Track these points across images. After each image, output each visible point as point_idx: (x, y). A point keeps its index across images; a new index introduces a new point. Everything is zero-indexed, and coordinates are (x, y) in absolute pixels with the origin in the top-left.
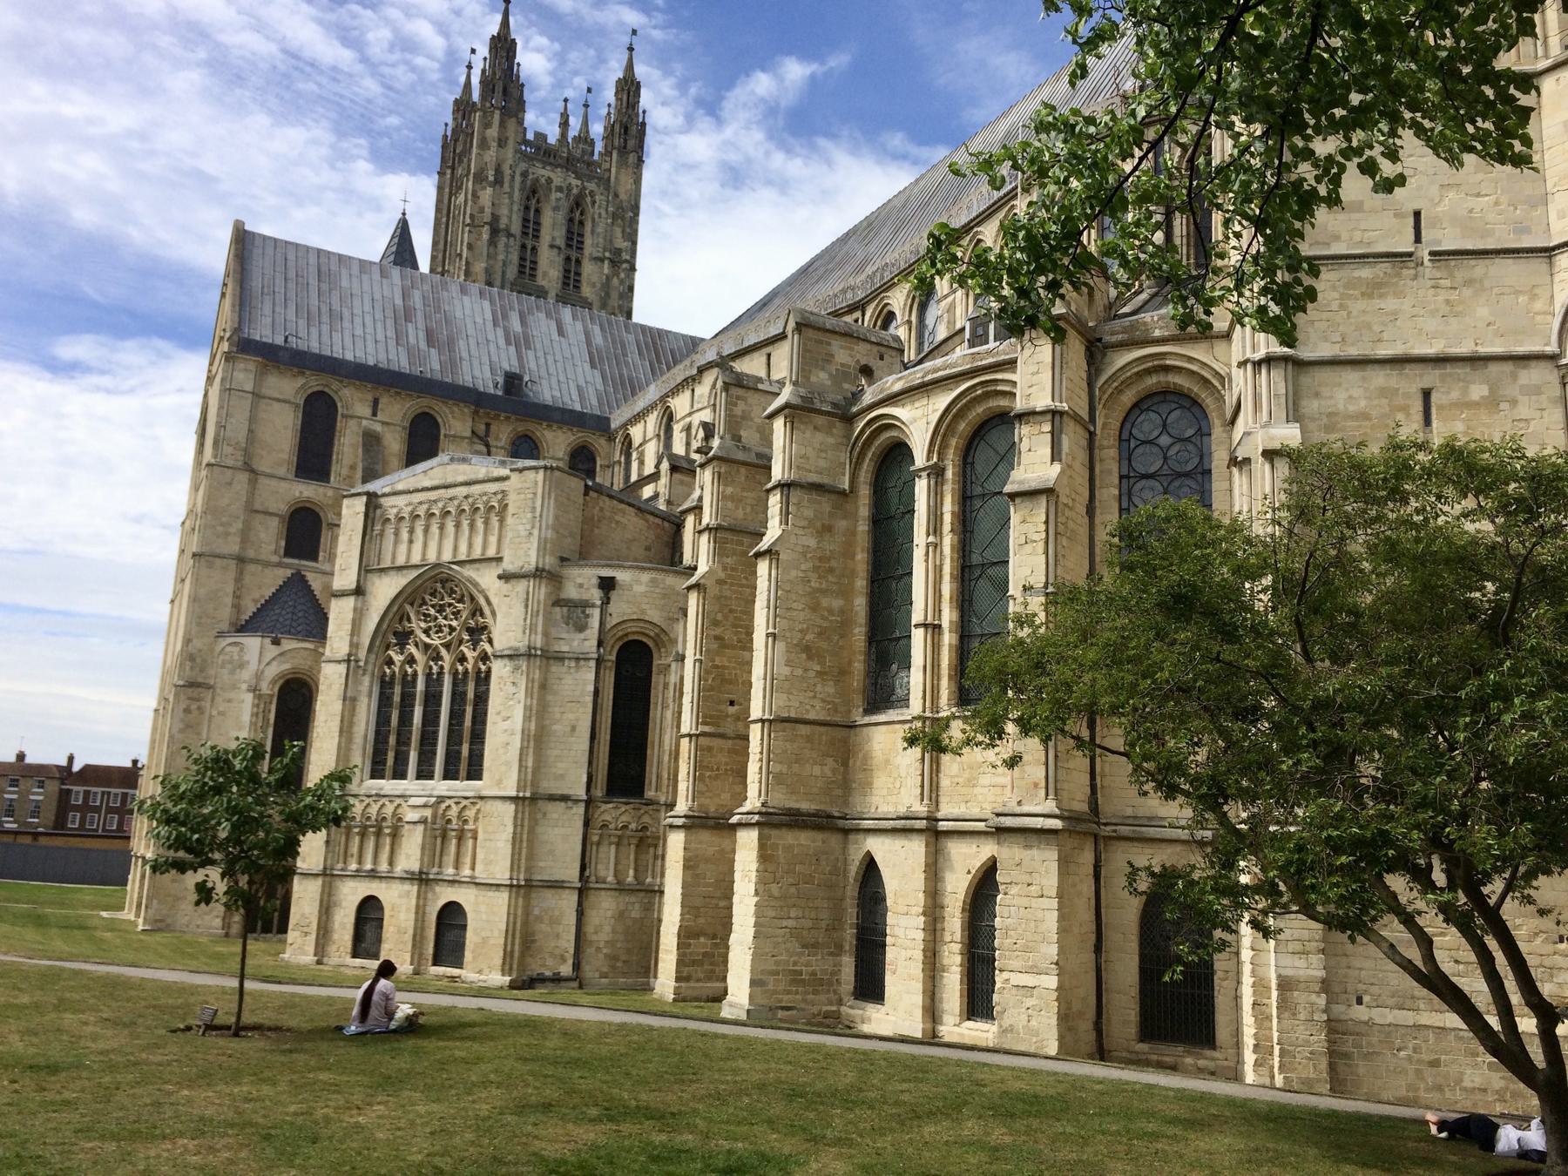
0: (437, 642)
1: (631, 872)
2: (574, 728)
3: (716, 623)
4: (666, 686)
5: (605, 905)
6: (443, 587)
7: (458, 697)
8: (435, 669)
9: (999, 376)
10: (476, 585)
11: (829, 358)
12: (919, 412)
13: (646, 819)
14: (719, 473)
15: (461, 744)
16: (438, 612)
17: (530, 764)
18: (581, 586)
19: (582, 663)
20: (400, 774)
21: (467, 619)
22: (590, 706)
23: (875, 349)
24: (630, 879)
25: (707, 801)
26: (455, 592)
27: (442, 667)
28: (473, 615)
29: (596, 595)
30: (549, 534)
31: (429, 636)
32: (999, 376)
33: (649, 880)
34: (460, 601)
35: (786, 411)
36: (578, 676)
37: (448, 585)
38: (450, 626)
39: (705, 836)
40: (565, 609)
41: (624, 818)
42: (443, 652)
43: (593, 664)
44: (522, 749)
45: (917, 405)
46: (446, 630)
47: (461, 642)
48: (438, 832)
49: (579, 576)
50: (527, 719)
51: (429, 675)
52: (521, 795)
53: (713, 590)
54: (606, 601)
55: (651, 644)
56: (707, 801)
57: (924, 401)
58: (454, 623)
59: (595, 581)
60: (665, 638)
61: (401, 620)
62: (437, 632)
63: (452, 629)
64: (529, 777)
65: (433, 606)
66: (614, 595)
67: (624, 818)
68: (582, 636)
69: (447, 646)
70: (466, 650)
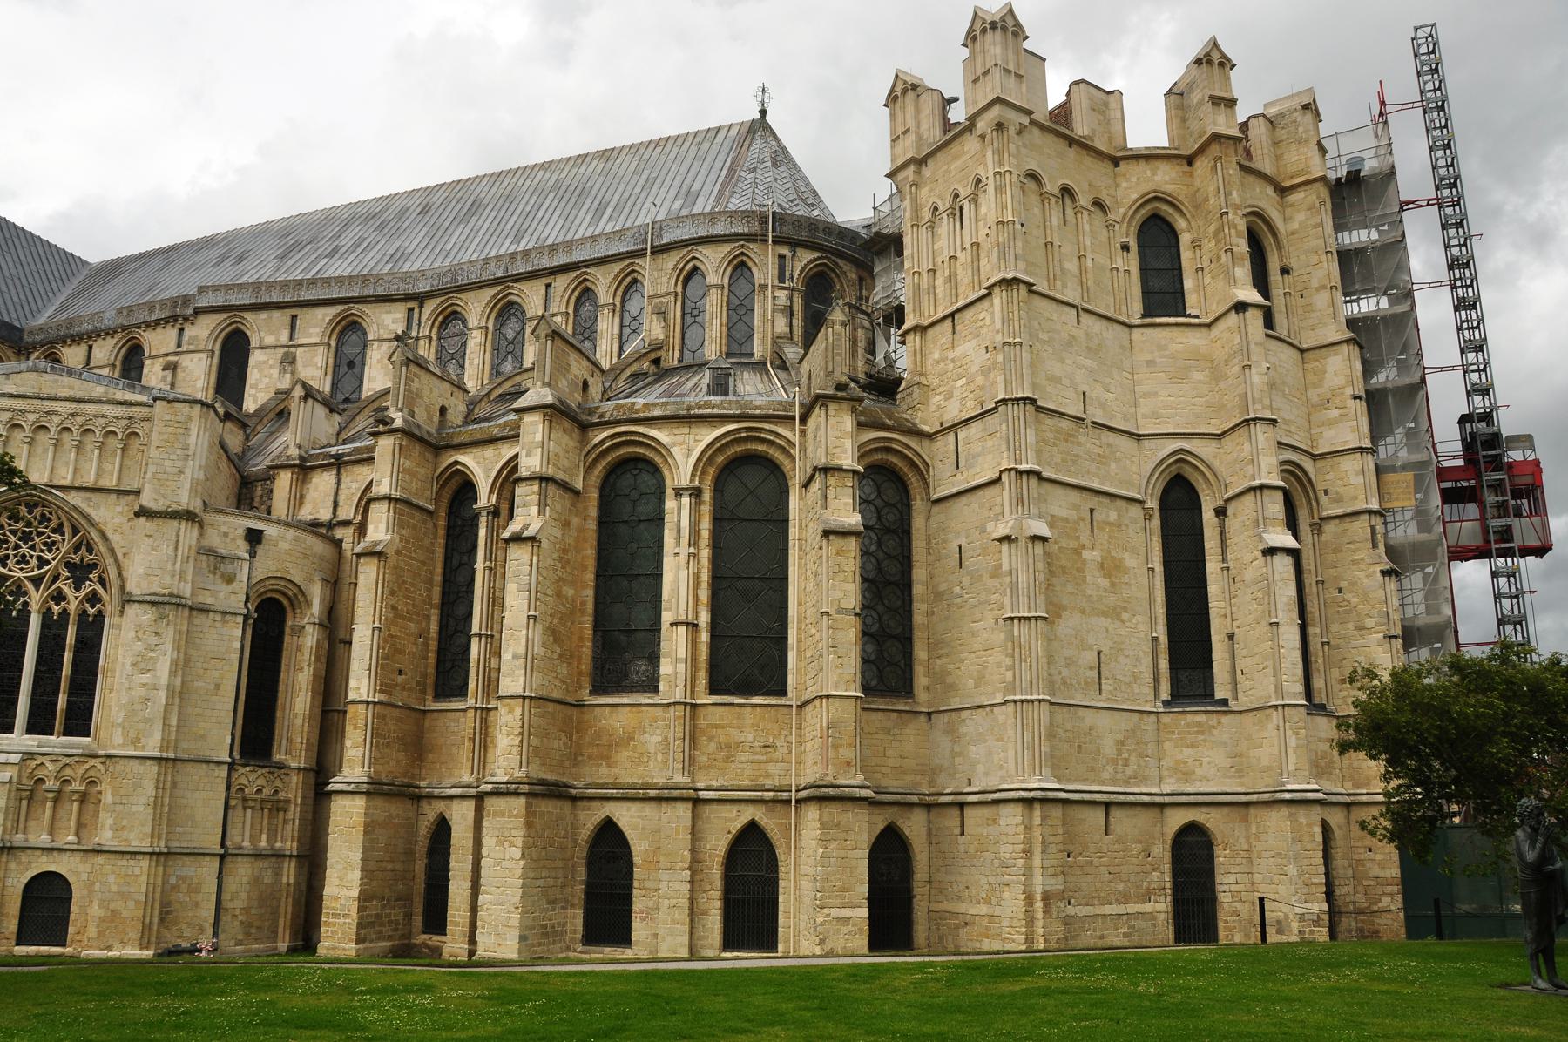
0: (21, 574)
1: (264, 837)
2: (218, 686)
3: (392, 593)
4: (299, 648)
5: (242, 871)
6: (30, 512)
9: (766, 426)
10: (87, 517)
11: (567, 368)
12: (679, 439)
13: (278, 783)
14: (401, 446)
15: (57, 693)
16: (20, 539)
17: (174, 722)
19: (228, 617)
21: (67, 552)
22: (236, 664)
23: (591, 366)
24: (263, 844)
25: (380, 768)
26: (49, 520)
27: (26, 604)
28: (77, 548)
29: (242, 549)
30: (202, 477)
32: (766, 426)
33: (278, 845)
34: (59, 529)
35: (548, 410)
37: (38, 511)
38: (39, 558)
39: (379, 802)
40: (212, 558)
41: (259, 782)
42: (30, 587)
43: (240, 619)
44: (167, 704)
45: (676, 431)
46: (34, 562)
47: (56, 578)
48: (25, 794)
50: (173, 673)
52: (165, 755)
53: (393, 560)
54: (253, 554)
55: (285, 602)
56: (380, 768)
57: (686, 430)
58: (48, 556)
59: (241, 532)
60: (302, 599)
62: (18, 563)
63: (42, 562)
64: (173, 736)
65: (14, 532)
66: (260, 550)
67: (259, 782)
68: (230, 588)
69: (36, 581)
70: (66, 589)
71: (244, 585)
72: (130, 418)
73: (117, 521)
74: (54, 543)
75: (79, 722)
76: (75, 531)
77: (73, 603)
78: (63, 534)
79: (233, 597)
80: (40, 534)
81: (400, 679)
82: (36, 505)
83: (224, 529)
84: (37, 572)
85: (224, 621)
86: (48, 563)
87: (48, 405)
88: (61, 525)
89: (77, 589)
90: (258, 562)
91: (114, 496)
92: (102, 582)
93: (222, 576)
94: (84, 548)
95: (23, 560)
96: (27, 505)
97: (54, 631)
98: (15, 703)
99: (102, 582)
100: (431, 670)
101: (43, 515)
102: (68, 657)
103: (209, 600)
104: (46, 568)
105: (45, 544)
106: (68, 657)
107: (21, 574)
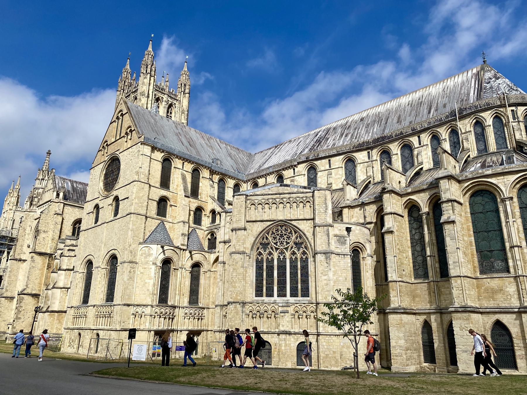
0: (282, 247)
7: (294, 267)
8: (282, 257)
18: (340, 230)
20: (270, 294)
28: (297, 238)
29: (346, 233)
31: (277, 245)
36: (345, 260)
46: (285, 243)
47: (292, 248)
49: (339, 226)
51: (279, 259)
61: (263, 239)
71: (349, 245)
72: (306, 197)
73: (307, 228)
74: (290, 237)
75: (306, 293)
76: (295, 232)
77: (299, 256)
78: (292, 234)
79: (347, 249)
80: (285, 235)
81: (404, 273)
82: (283, 226)
83: (339, 228)
84: (286, 246)
85: (344, 257)
86: (289, 243)
87: (282, 196)
88: (291, 231)
89: (299, 250)
90: (351, 238)
91: (305, 221)
92: (306, 248)
93: (342, 243)
94: (299, 238)
95: (282, 243)
96: (280, 226)
97: (293, 264)
98: (285, 287)
99: (306, 248)
100: (412, 269)
101: (285, 229)
102: (299, 272)
103: (340, 251)
104: (288, 245)
105: (287, 237)
106: (299, 272)
107: (282, 247)
